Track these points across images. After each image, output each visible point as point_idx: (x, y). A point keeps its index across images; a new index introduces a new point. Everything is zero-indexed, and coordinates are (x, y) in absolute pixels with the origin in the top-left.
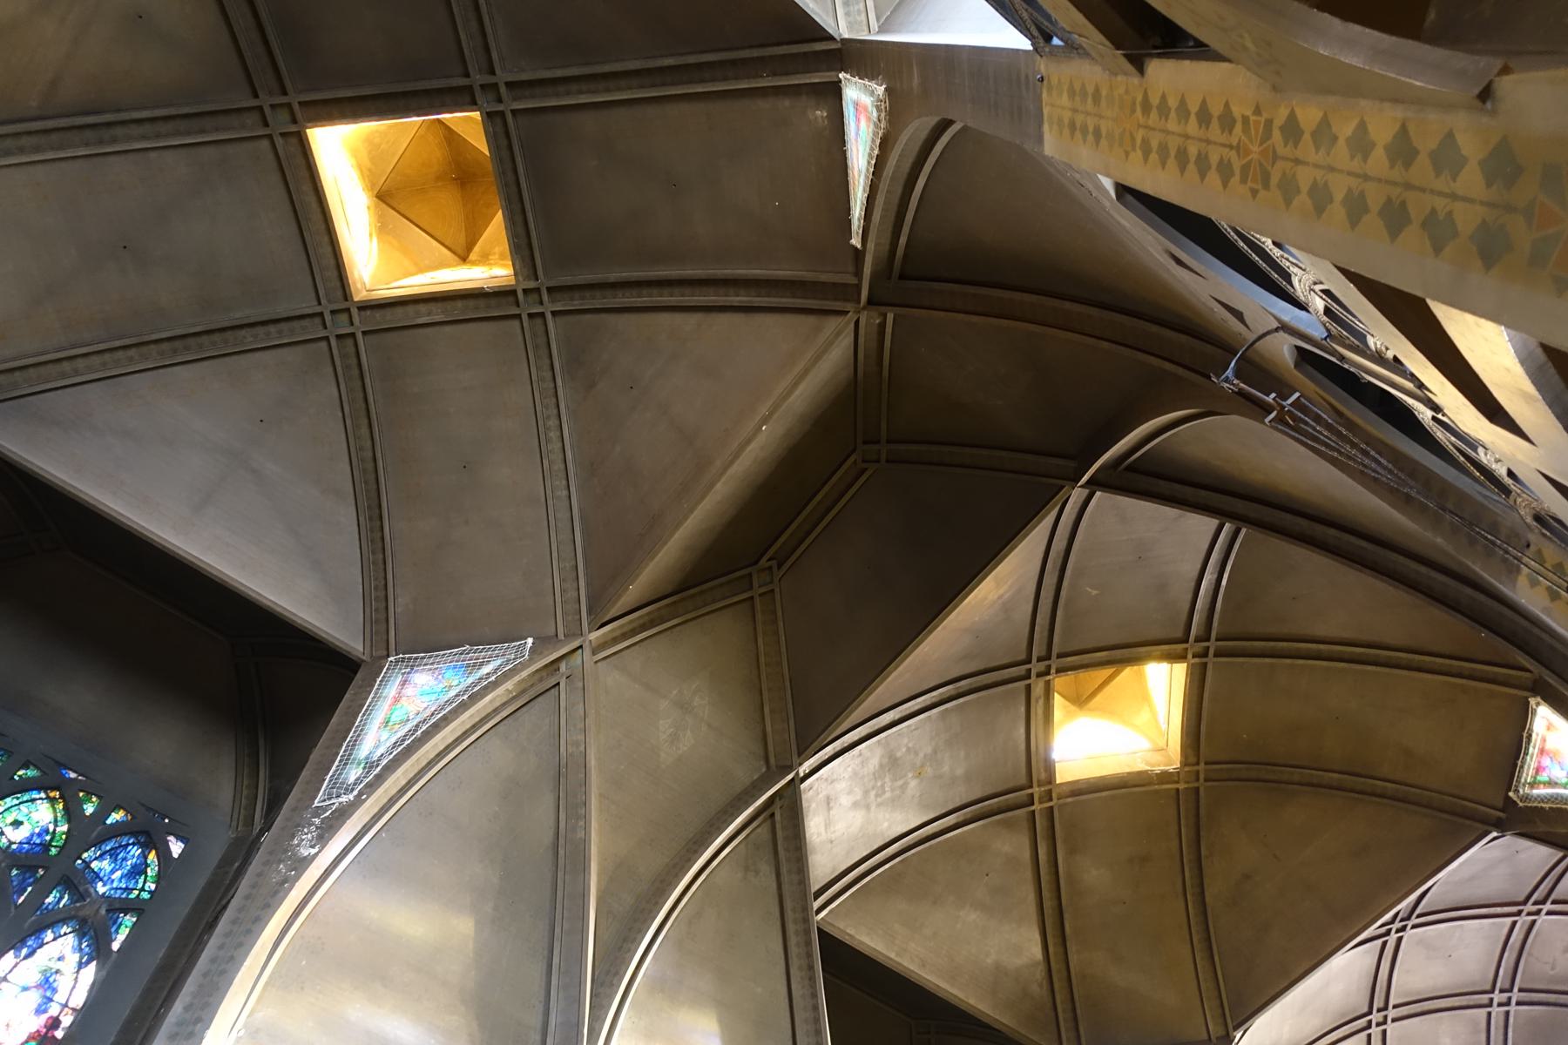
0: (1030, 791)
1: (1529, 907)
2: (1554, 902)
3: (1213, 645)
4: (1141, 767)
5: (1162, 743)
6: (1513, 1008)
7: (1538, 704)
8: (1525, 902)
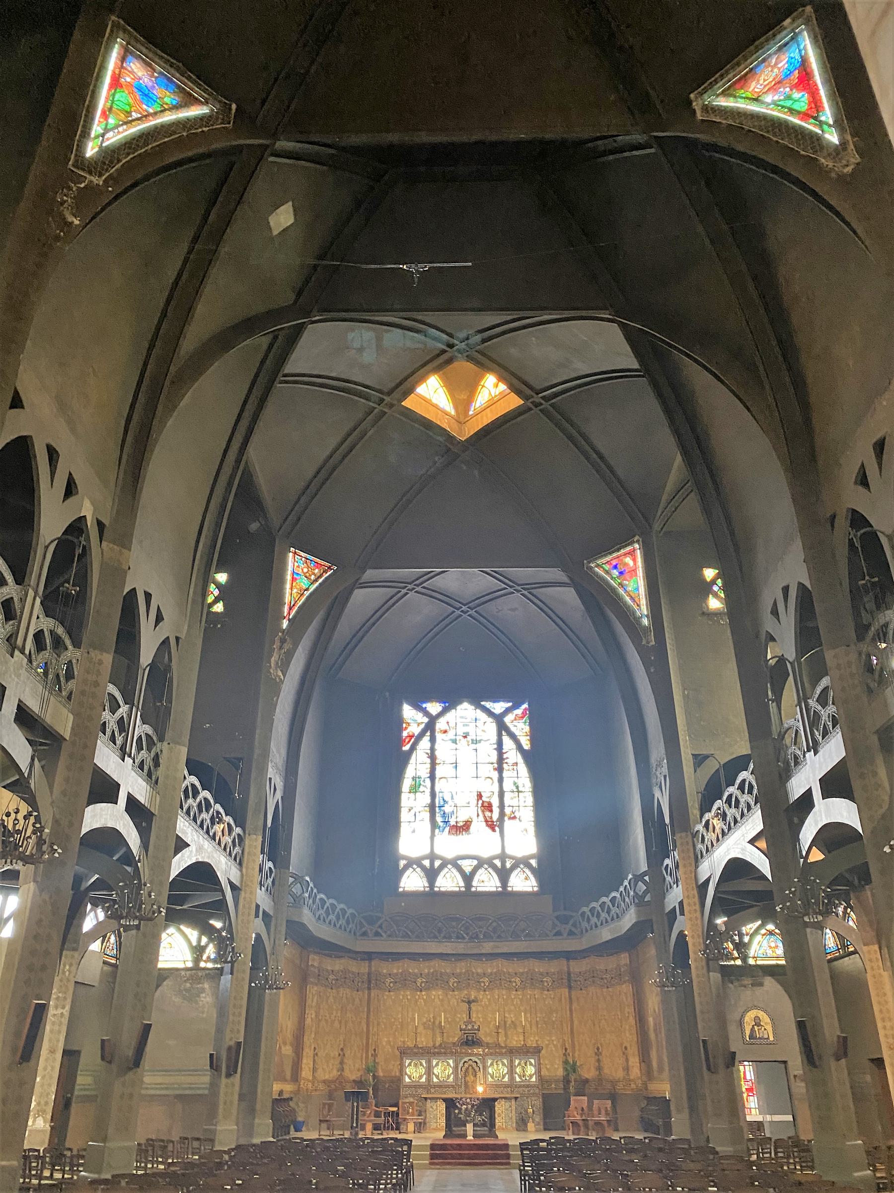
0: (385, 397)
1: (519, 588)
2: (530, 593)
3: (546, 405)
4: (445, 426)
5: (462, 419)
6: (464, 615)
7: (638, 541)
8: (519, 585)
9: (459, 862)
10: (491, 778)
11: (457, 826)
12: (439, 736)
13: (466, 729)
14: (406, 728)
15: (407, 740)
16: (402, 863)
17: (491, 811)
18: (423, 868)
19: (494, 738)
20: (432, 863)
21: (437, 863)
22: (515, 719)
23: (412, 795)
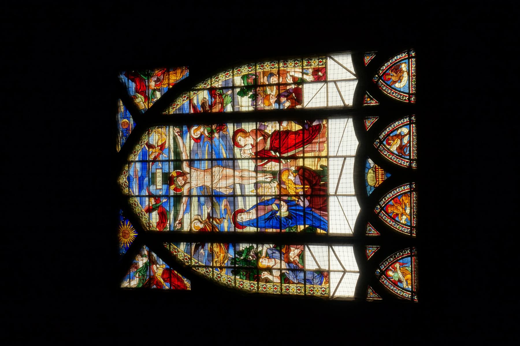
9: (370, 192)
10: (235, 133)
11: (312, 196)
12: (171, 225)
13: (159, 179)
14: (158, 283)
15: (177, 283)
16: (372, 295)
17: (287, 133)
18: (379, 258)
19: (173, 131)
20: (373, 241)
21: (372, 232)
22: (143, 93)
23: (265, 275)
